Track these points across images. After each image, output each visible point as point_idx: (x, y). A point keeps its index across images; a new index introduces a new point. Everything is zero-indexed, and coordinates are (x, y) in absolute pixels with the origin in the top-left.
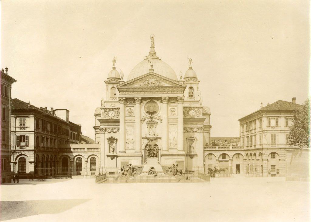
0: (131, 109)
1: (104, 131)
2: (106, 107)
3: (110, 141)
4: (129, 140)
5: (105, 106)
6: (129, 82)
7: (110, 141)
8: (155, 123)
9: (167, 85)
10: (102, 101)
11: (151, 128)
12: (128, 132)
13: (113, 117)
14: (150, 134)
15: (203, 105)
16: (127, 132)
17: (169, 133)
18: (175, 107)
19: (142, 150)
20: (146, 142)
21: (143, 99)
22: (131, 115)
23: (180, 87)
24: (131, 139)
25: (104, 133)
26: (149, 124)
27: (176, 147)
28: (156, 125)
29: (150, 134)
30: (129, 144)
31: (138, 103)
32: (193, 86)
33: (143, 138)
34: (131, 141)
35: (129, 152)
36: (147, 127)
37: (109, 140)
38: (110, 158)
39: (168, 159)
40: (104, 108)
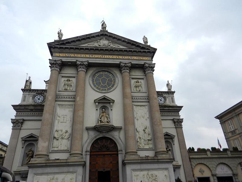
0: (69, 81)
1: (20, 125)
2: (32, 88)
3: (27, 143)
4: (60, 132)
6: (70, 41)
7: (27, 143)
8: (110, 103)
10: (27, 81)
11: (104, 109)
12: (59, 117)
14: (101, 121)
15: (173, 90)
16: (58, 118)
17: (136, 120)
18: (142, 81)
19: (84, 153)
20: (93, 135)
21: (90, 66)
22: (68, 89)
24: (64, 131)
25: (19, 127)
26: (101, 104)
27: (151, 146)
28: (111, 106)
29: (101, 121)
30: (60, 140)
31: (83, 69)
33: (88, 129)
34: (64, 134)
35: (53, 157)
36: (95, 109)
37: (25, 141)
39: (142, 170)
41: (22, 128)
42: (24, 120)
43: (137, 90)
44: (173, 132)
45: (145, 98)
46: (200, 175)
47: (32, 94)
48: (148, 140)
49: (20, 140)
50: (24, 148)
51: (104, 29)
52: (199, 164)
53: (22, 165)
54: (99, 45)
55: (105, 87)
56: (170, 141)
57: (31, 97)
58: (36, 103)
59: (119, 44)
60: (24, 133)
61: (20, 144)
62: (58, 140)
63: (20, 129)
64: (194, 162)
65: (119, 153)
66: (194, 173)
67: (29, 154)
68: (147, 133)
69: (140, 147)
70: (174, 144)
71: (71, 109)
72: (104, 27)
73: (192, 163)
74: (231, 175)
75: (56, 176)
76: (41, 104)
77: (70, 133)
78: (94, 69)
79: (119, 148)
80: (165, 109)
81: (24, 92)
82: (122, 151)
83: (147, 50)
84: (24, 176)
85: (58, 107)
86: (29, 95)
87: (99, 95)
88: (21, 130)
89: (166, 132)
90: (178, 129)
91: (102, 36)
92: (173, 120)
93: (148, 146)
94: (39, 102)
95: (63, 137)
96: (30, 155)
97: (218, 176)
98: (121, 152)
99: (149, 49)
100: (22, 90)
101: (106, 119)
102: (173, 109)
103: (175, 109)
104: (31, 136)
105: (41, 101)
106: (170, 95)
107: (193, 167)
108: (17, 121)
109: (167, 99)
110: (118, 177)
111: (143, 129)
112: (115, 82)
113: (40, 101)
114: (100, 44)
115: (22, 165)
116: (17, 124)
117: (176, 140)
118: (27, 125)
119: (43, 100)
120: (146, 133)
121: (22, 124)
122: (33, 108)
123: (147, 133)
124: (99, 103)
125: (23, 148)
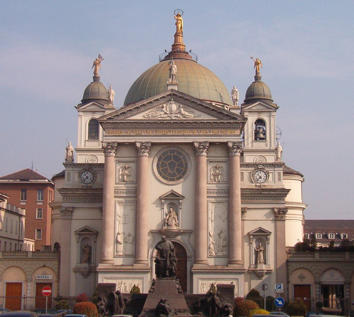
5: (73, 160)
8: (179, 199)
9: (205, 117)
13: (89, 185)
23: (232, 121)
25: (70, 217)
29: (167, 224)
32: (265, 117)
34: (128, 238)
38: (78, 274)
40: (70, 165)
41: (73, 218)
42: (73, 208)
43: (215, 181)
44: (269, 226)
45: (225, 192)
46: (299, 282)
47: (77, 169)
48: (222, 246)
49: (73, 232)
50: (80, 242)
51: (173, 77)
52: (301, 268)
53: (81, 263)
54: (166, 113)
55: (174, 175)
56: (264, 238)
57: (77, 175)
58: (85, 185)
59: (195, 109)
60: (77, 225)
61: (74, 239)
62: (121, 244)
63: (71, 219)
64: (294, 266)
65: (188, 259)
66: (290, 280)
67: (86, 250)
68: (222, 238)
69: (212, 254)
70: (269, 244)
71: (133, 207)
72: (173, 75)
73: (289, 267)
74: (343, 284)
75: (124, 281)
76: (90, 185)
77: (133, 236)
78: (159, 148)
79: (188, 254)
80: (264, 193)
81: (67, 167)
82: (191, 258)
83: (232, 121)
84: (85, 274)
85: (117, 204)
86: (73, 171)
87: (164, 189)
88: (73, 221)
89: (260, 227)
90: (279, 223)
91: (169, 97)
92: (273, 209)
93: (222, 253)
94: (88, 182)
95: (127, 241)
96: (88, 252)
97: (322, 283)
98: (190, 259)
99: (236, 119)
100: (64, 164)
101: (174, 221)
102: (276, 193)
103: (278, 193)
104: (86, 230)
105: (91, 181)
106: (276, 169)
107: (290, 272)
108: (66, 210)
109: (271, 175)
110: (186, 283)
111: (218, 233)
112: (186, 168)
113: (88, 181)
114: (166, 112)
115: (81, 263)
116: (66, 213)
117: (272, 238)
118: (77, 214)
119: (92, 178)
120: (221, 238)
121: (72, 213)
122: (82, 192)
123: (222, 238)
124: (165, 199)
125: (78, 242)
